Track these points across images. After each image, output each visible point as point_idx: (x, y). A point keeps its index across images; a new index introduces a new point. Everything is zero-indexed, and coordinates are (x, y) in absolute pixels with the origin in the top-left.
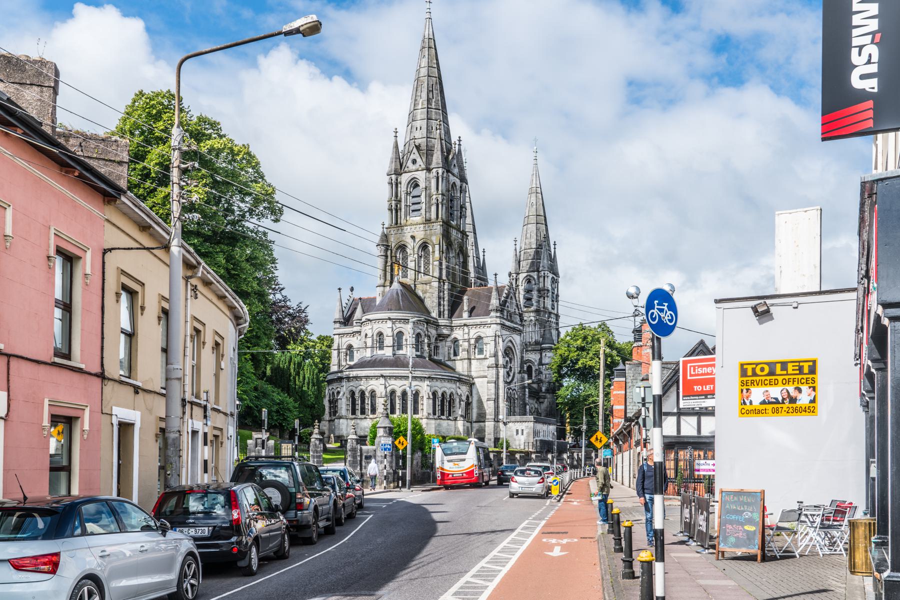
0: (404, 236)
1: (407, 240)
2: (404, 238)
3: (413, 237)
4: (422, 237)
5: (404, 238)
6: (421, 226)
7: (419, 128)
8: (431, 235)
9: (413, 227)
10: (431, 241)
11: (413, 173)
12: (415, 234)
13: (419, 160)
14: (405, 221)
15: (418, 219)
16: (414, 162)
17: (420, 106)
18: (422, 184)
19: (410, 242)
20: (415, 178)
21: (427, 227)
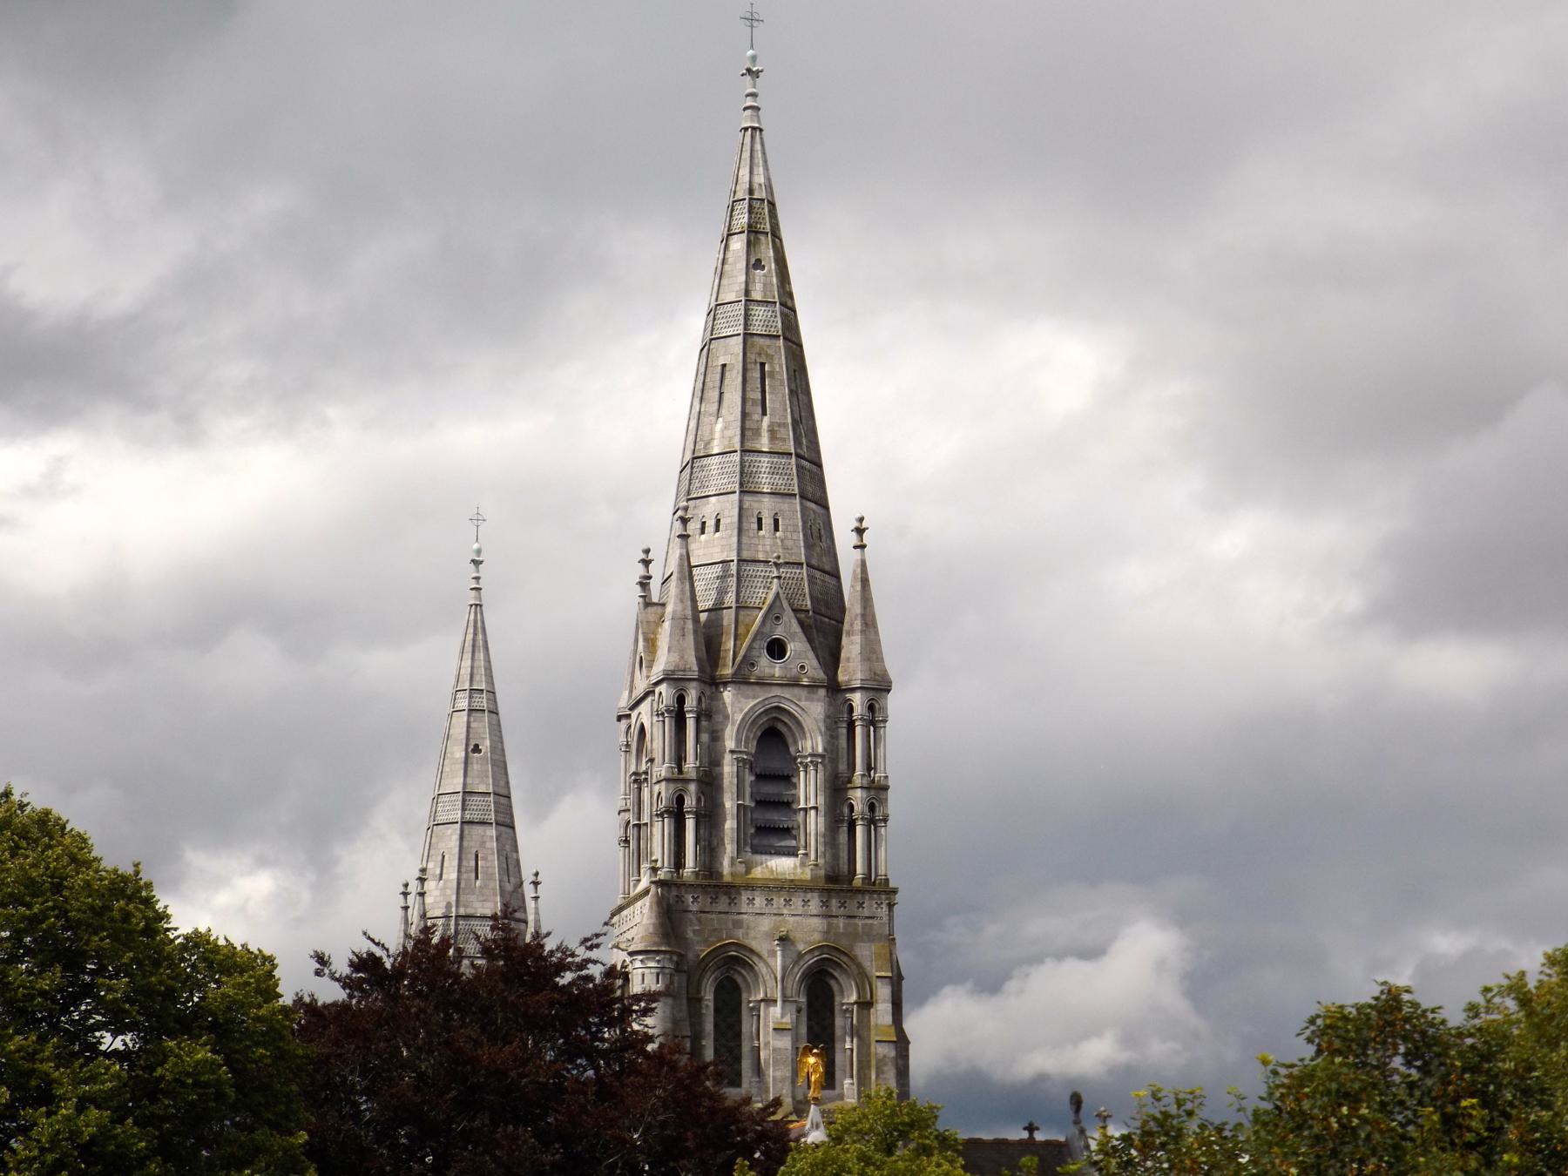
0: (738, 924)
1: (754, 945)
2: (740, 933)
3: (784, 940)
4: (816, 937)
5: (740, 933)
6: (809, 896)
7: (768, 522)
8: (855, 937)
9: (779, 901)
10: (853, 959)
11: (777, 691)
12: (790, 923)
13: (797, 647)
14: (741, 869)
15: (783, 866)
16: (777, 649)
17: (764, 443)
18: (812, 742)
19: (765, 954)
20: (778, 708)
21: (834, 902)
